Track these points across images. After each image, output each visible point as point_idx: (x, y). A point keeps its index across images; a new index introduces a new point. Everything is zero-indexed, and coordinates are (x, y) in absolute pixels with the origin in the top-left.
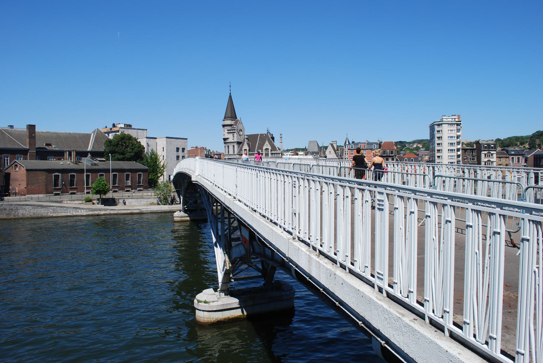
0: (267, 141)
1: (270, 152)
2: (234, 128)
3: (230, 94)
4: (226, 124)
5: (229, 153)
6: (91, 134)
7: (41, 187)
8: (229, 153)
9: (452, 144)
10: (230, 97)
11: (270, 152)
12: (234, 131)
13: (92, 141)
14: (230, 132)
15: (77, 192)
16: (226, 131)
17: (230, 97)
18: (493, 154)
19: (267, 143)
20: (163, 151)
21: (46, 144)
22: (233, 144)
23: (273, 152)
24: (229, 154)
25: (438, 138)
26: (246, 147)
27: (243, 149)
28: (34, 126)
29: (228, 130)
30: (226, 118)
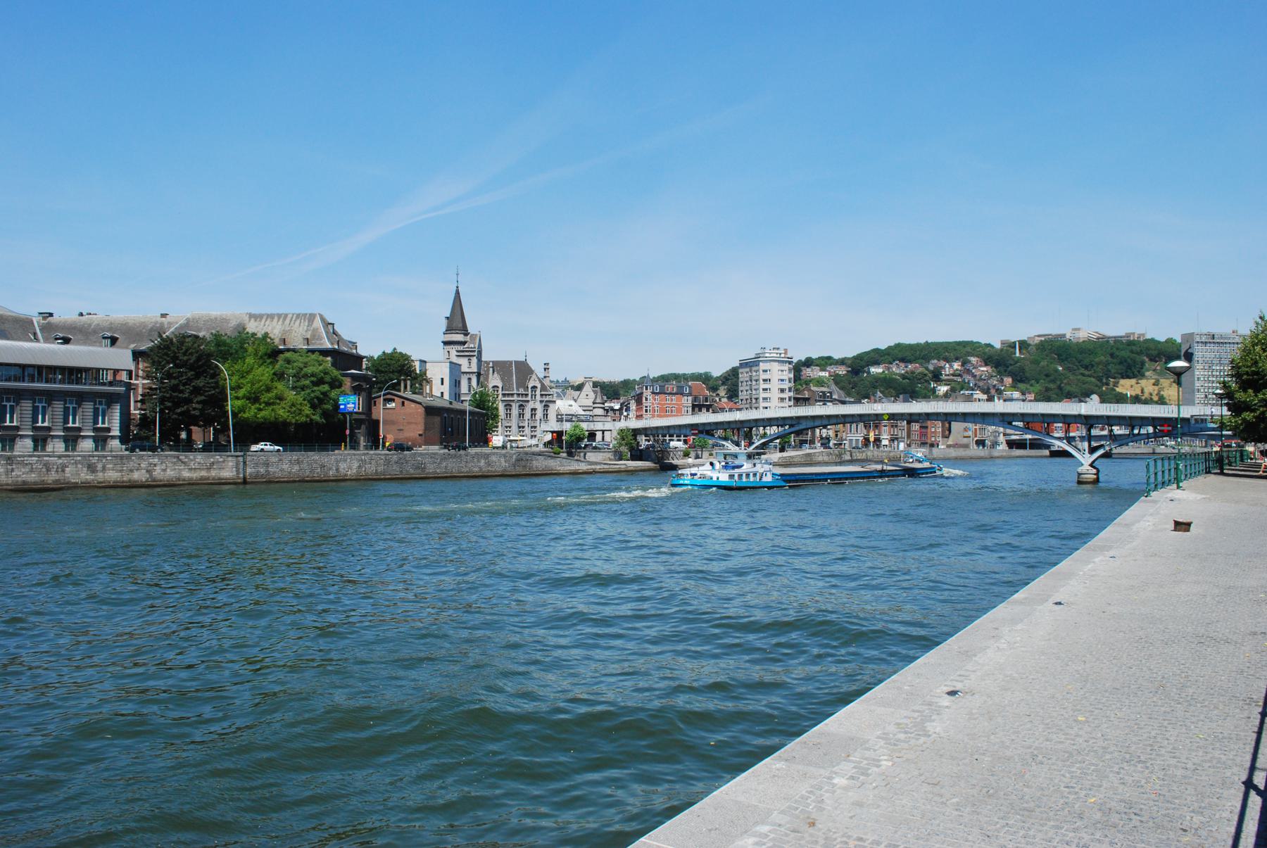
1: (500, 392)
9: (782, 391)
10: (457, 293)
11: (538, 392)
16: (454, 353)
17: (457, 293)
19: (534, 376)
20: (442, 384)
22: (468, 376)
23: (543, 393)
25: (764, 380)
29: (457, 351)
30: (450, 330)
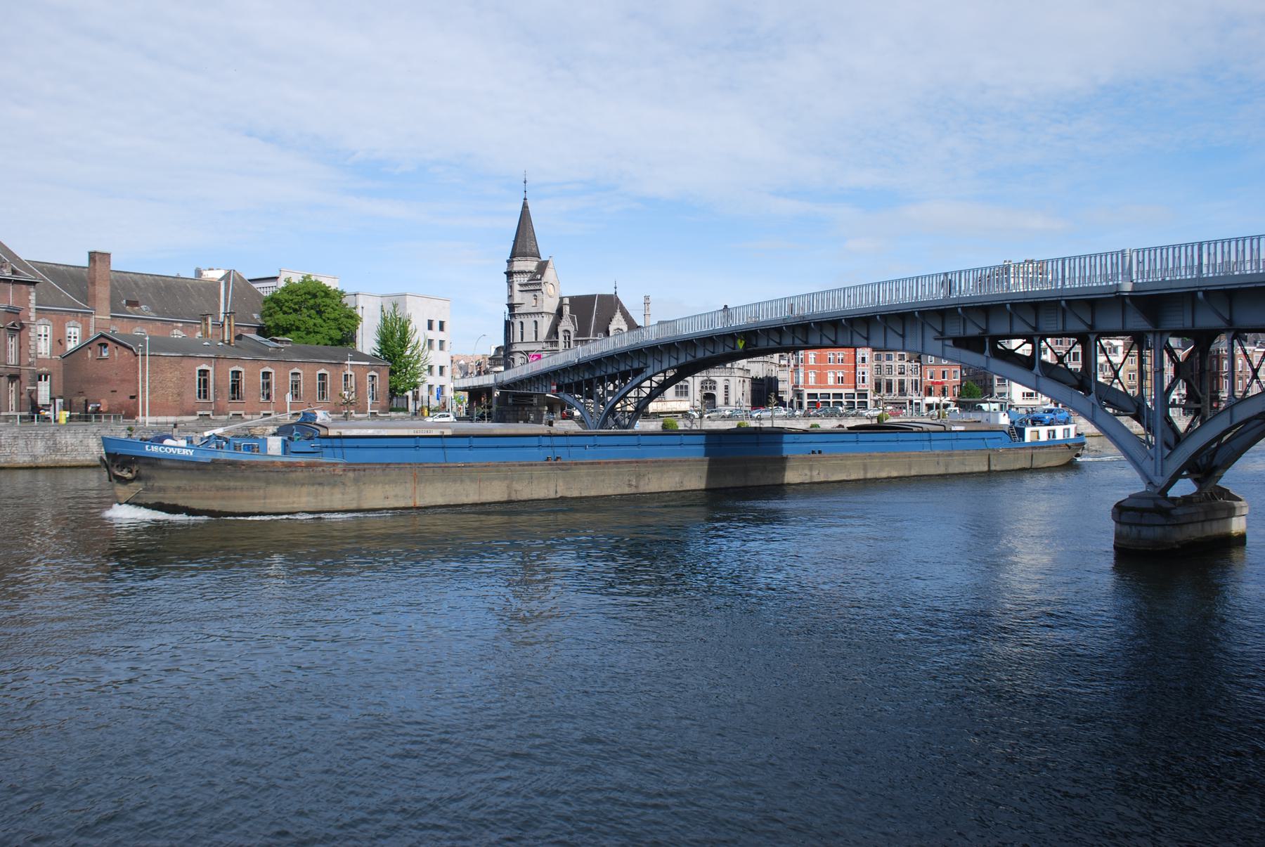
0: (618, 310)
2: (538, 280)
3: (525, 199)
4: (516, 269)
5: (522, 339)
6: (220, 283)
7: (170, 398)
8: (522, 339)
10: (525, 206)
12: (538, 288)
13: (226, 299)
14: (527, 288)
15: (245, 414)
17: (525, 206)
18: (1117, 347)
19: (618, 316)
21: (127, 301)
24: (524, 341)
26: (566, 324)
27: (560, 330)
28: (109, 255)
29: (521, 285)
